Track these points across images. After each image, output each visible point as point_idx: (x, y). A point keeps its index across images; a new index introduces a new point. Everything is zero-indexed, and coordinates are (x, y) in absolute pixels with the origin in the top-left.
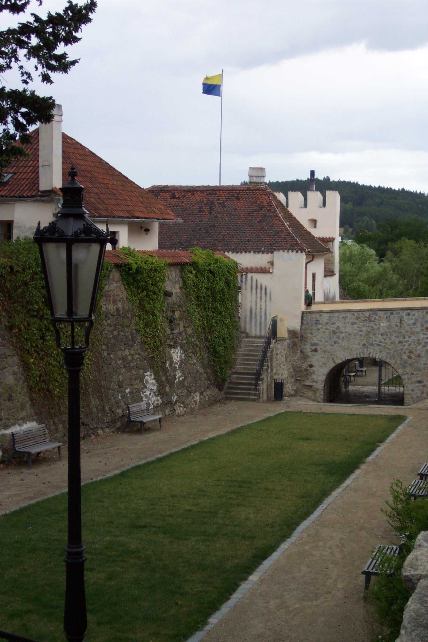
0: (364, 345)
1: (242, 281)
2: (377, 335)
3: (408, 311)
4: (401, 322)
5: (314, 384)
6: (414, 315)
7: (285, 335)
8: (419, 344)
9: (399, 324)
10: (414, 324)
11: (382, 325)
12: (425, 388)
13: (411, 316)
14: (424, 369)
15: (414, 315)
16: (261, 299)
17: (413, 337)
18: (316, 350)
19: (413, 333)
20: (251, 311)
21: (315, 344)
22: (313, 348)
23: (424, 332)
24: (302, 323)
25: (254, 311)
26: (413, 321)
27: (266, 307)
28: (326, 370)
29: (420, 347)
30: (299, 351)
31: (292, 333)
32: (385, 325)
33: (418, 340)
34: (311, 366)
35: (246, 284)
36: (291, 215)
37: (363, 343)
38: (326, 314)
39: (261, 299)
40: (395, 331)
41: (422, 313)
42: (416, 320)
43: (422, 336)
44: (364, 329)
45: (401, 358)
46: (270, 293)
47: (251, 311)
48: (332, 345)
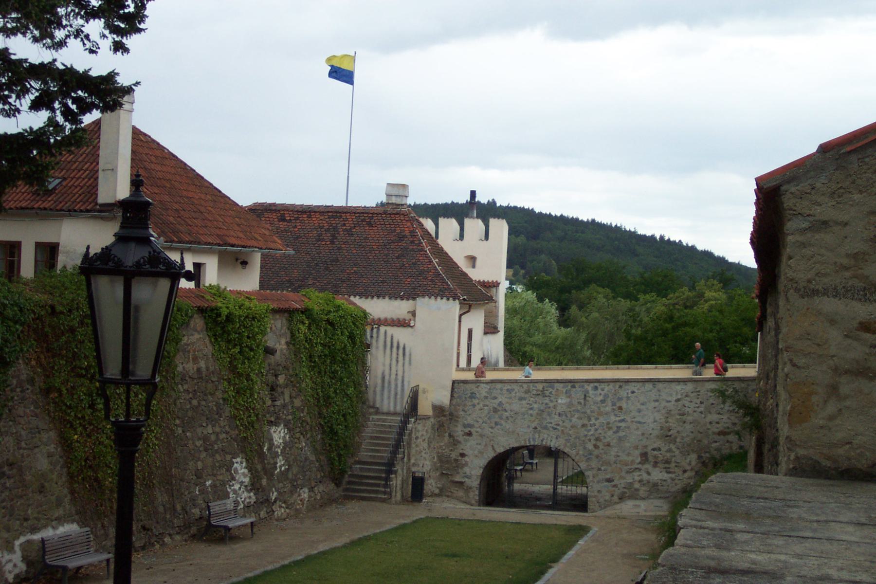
0: (536, 428)
1: (372, 337)
2: (553, 415)
3: (596, 384)
4: (585, 399)
5: (466, 480)
6: (603, 390)
7: (430, 413)
8: (610, 428)
9: (582, 401)
10: (603, 401)
11: (560, 401)
12: (616, 489)
13: (599, 391)
14: (615, 462)
15: (603, 390)
16: (397, 361)
17: (602, 420)
18: (470, 434)
19: (600, 414)
20: (383, 378)
21: (470, 426)
22: (467, 430)
23: (616, 412)
24: (452, 396)
25: (387, 378)
26: (601, 398)
27: (404, 372)
28: (483, 462)
29: (610, 433)
30: (447, 434)
31: (439, 410)
32: (564, 401)
33: (608, 423)
34: (463, 455)
35: (377, 341)
36: (442, 249)
37: (534, 425)
38: (484, 385)
39: (397, 361)
40: (578, 411)
41: (614, 387)
42: (606, 396)
43: (613, 418)
44: (536, 406)
45: (585, 448)
46: (410, 355)
47: (383, 378)
48: (492, 428)
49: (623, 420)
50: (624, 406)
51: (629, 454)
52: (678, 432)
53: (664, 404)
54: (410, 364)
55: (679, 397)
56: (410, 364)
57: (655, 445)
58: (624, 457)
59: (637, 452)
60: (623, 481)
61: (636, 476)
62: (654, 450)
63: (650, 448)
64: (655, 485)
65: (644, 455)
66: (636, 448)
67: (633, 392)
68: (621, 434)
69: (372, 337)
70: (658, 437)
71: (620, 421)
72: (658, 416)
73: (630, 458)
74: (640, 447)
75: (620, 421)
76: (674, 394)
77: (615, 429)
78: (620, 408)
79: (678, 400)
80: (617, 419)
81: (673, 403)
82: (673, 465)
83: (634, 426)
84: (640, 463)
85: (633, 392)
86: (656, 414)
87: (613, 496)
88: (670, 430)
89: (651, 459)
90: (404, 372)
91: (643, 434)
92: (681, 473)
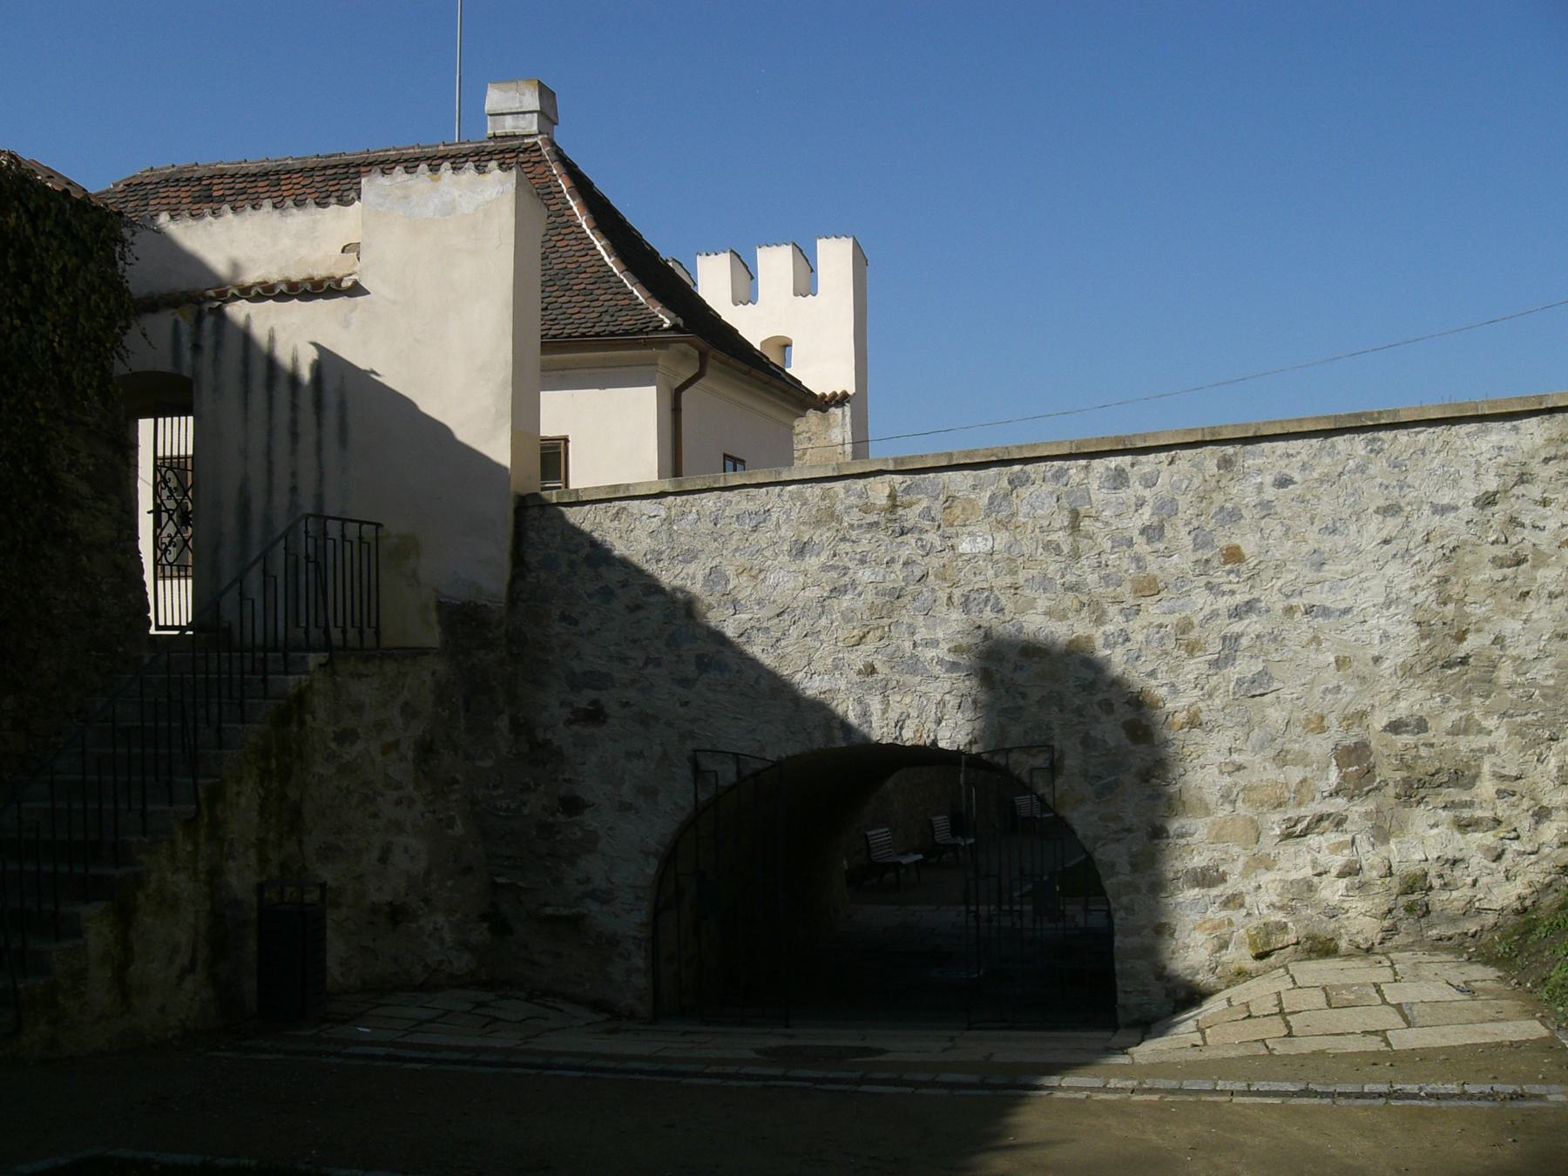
0: (871, 670)
1: (197, 348)
2: (941, 610)
3: (1113, 462)
4: (1074, 526)
5: (594, 907)
6: (1149, 482)
7: (433, 637)
8: (1192, 649)
9: (1061, 537)
10: (1153, 532)
11: (965, 546)
12: (1238, 915)
13: (1136, 488)
14: (1227, 797)
15: (1149, 482)
16: (294, 435)
17: (1153, 611)
18: (595, 715)
19: (1149, 588)
20: (244, 507)
21: (599, 680)
22: (583, 700)
23: (1219, 577)
24: (518, 559)
25: (258, 505)
26: (1146, 516)
27: (321, 480)
28: (656, 827)
29: (1194, 667)
30: (503, 723)
31: (463, 620)
32: (982, 546)
33: (1185, 627)
34: (573, 805)
35: (216, 360)
36: (653, 254)
37: (858, 659)
38: (648, 506)
39: (294, 435)
40: (1045, 583)
41: (1198, 466)
42: (1167, 508)
43: (1201, 601)
44: (865, 575)
45: (1087, 742)
46: (342, 405)
47: (244, 507)
48: (684, 682)
49: (1250, 606)
50: (1249, 544)
51: (1281, 759)
52: (1498, 640)
53: (1424, 521)
54: (343, 441)
55: (1491, 484)
56: (343, 441)
57: (1402, 709)
58: (1263, 772)
59: (1319, 746)
60: (1266, 878)
61: (1324, 849)
62: (1395, 727)
63: (1379, 721)
64: (1415, 884)
65: (1355, 756)
66: (1318, 725)
67: (1284, 482)
68: (1245, 667)
69: (197, 348)
70: (1407, 670)
71: (1237, 613)
72: (1400, 575)
73: (1295, 774)
74: (1332, 720)
75: (1237, 613)
76: (1467, 473)
77: (1215, 647)
78: (1233, 555)
79: (1487, 501)
80: (1224, 603)
81: (1467, 511)
82: (1486, 788)
83: (1302, 627)
84: (1335, 793)
85: (1284, 482)
86: (1392, 569)
87: (1224, 946)
88: (1461, 637)
89: (1388, 772)
90: (321, 480)
91: (1341, 663)
92: (1525, 823)
